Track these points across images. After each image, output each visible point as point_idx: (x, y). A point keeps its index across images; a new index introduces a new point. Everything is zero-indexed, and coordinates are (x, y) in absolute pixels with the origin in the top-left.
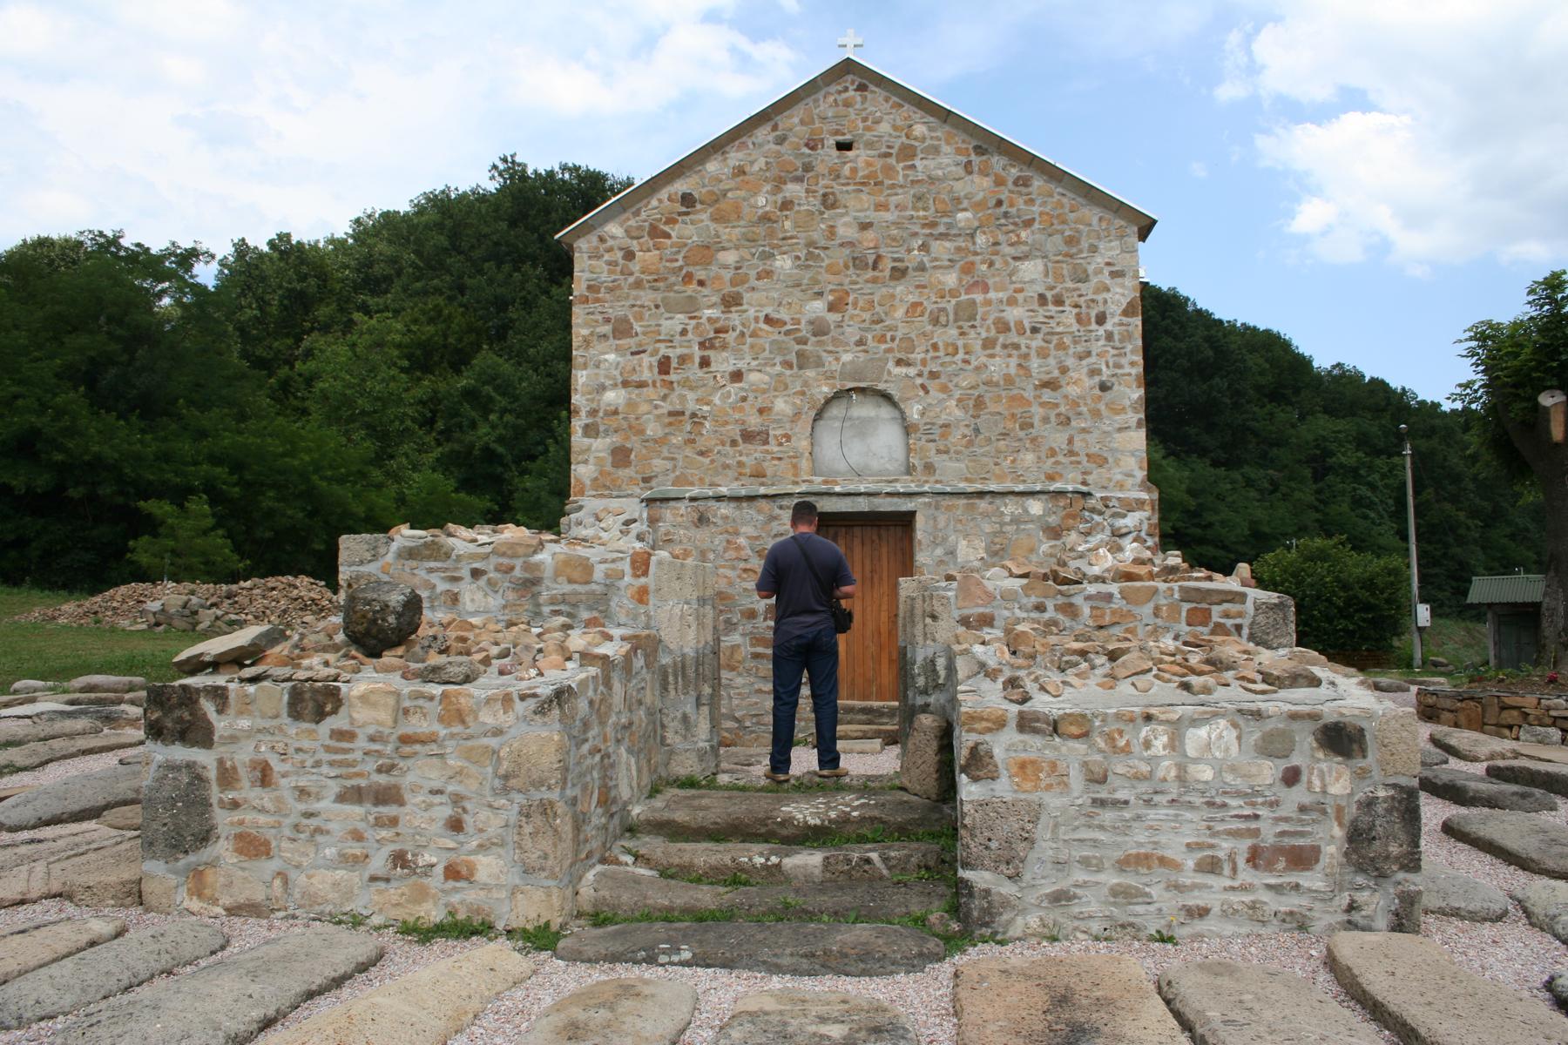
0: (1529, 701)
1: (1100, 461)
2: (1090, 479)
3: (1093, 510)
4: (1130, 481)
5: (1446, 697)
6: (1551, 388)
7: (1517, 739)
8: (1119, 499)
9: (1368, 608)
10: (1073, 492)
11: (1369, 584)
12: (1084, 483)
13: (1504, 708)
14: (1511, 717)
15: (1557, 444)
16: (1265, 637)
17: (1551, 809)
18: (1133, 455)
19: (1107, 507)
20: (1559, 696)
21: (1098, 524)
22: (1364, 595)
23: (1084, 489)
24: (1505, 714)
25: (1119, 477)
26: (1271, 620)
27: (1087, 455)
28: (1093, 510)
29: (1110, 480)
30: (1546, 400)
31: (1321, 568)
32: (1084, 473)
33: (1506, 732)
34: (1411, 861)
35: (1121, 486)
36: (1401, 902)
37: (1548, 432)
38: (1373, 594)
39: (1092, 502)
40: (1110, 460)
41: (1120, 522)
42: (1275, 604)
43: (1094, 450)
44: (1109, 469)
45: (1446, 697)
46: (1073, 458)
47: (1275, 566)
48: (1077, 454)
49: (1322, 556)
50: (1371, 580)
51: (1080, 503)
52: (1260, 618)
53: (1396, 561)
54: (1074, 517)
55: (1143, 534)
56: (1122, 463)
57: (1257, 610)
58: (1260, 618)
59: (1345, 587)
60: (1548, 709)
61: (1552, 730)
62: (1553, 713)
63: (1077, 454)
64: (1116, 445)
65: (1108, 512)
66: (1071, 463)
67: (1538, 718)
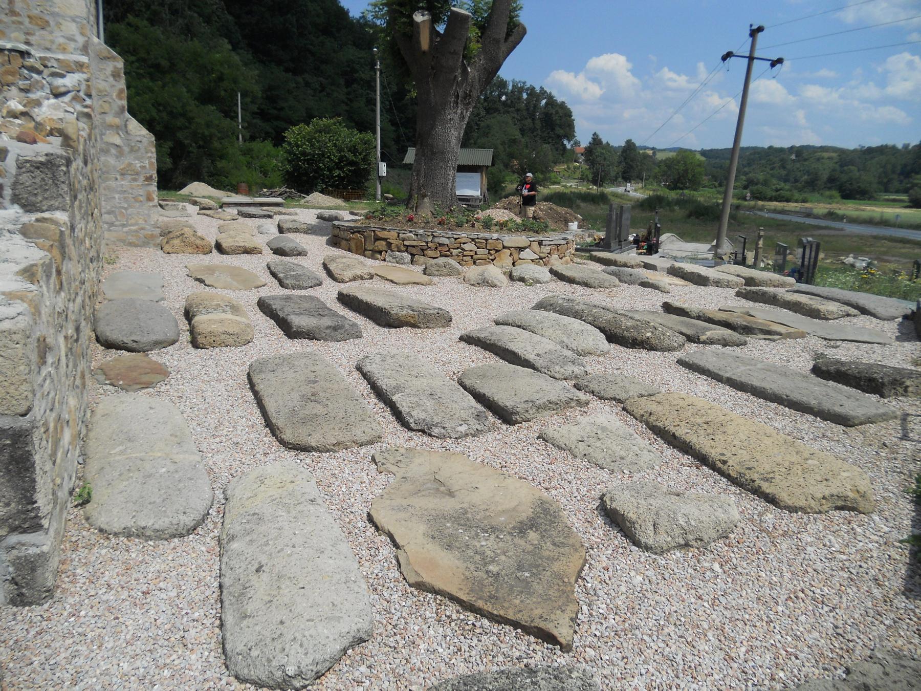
0: (392, 235)
1: (44, 25)
2: (32, 39)
3: (32, 69)
4: (72, 45)
5: (344, 230)
6: (422, 8)
7: (384, 260)
8: (57, 60)
9: (352, 163)
10: (10, 50)
11: (354, 150)
12: (27, 43)
13: (377, 239)
14: (381, 245)
15: (424, 52)
16: (33, 199)
17: (357, 337)
18: (74, 21)
19: (46, 66)
20: (411, 232)
21: (37, 82)
22: (350, 156)
23: (23, 47)
24: (377, 243)
25: (62, 40)
26: (38, 180)
27: (29, 17)
28: (32, 69)
29: (52, 42)
30: (419, 18)
31: (325, 137)
32: (27, 34)
33: (379, 256)
34: (25, 521)
35: (64, 50)
36: (17, 569)
37: (419, 43)
38: (355, 155)
39: (30, 62)
40: (52, 23)
41: (59, 82)
42: (41, 163)
43: (36, 12)
44: (51, 32)
45: (344, 230)
46: (15, 18)
47: (298, 135)
48: (18, 15)
49: (326, 130)
50: (354, 147)
51: (18, 61)
52: (24, 178)
53: (368, 136)
54: (13, 74)
55: (82, 94)
56: (63, 28)
57: (19, 168)
58: (24, 178)
59: (340, 150)
60: (403, 240)
61: (405, 254)
62: (406, 243)
63: (18, 15)
64: (57, 10)
65: (46, 72)
66: (14, 22)
67: (397, 247)
